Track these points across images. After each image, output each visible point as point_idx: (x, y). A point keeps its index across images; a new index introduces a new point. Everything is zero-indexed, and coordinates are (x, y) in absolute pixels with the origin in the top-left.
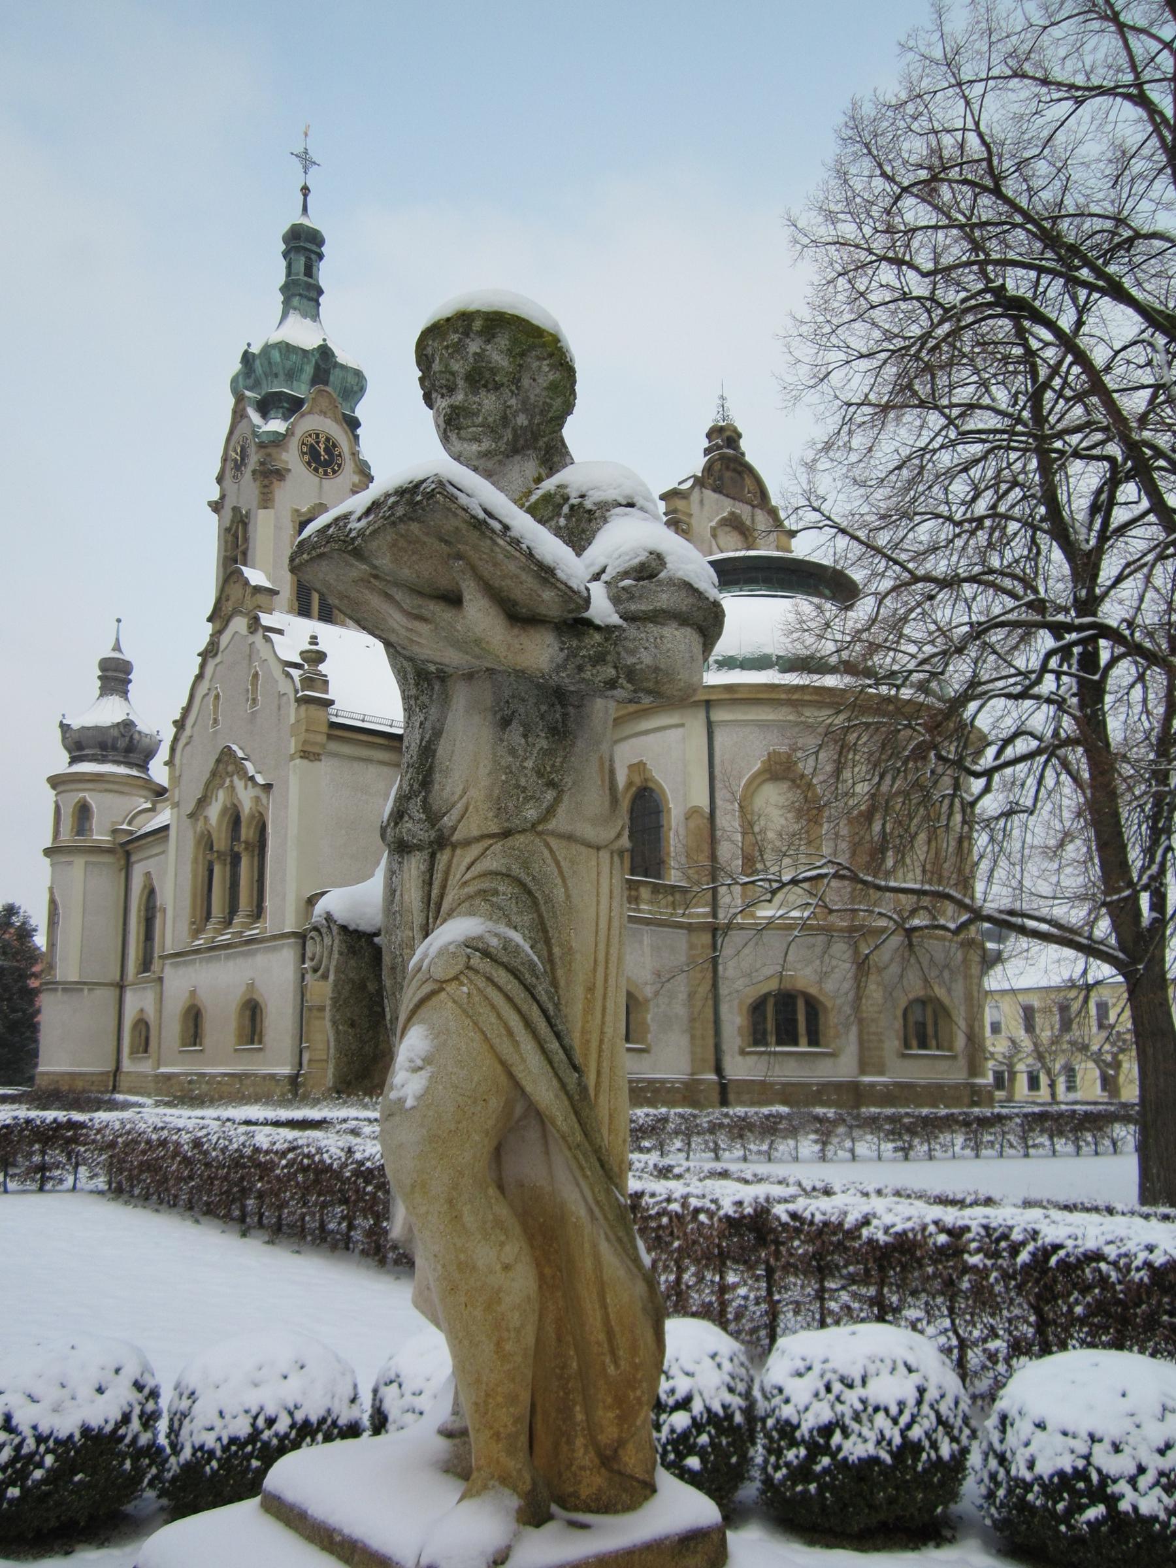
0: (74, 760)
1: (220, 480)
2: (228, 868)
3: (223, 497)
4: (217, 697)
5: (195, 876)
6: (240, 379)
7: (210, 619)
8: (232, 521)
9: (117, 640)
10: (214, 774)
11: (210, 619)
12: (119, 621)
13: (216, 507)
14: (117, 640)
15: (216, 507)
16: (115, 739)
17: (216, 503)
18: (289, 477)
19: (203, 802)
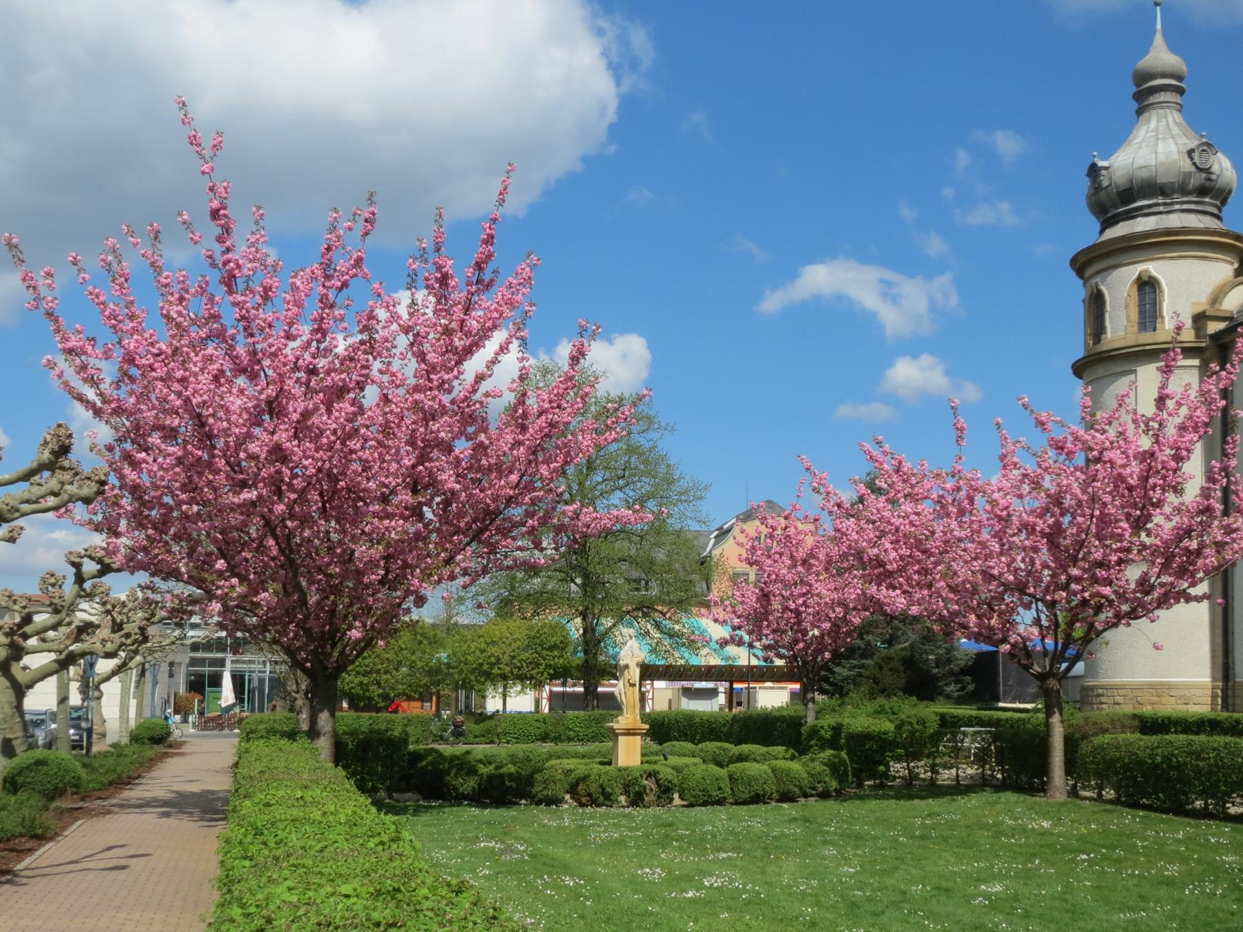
0: (1107, 224)
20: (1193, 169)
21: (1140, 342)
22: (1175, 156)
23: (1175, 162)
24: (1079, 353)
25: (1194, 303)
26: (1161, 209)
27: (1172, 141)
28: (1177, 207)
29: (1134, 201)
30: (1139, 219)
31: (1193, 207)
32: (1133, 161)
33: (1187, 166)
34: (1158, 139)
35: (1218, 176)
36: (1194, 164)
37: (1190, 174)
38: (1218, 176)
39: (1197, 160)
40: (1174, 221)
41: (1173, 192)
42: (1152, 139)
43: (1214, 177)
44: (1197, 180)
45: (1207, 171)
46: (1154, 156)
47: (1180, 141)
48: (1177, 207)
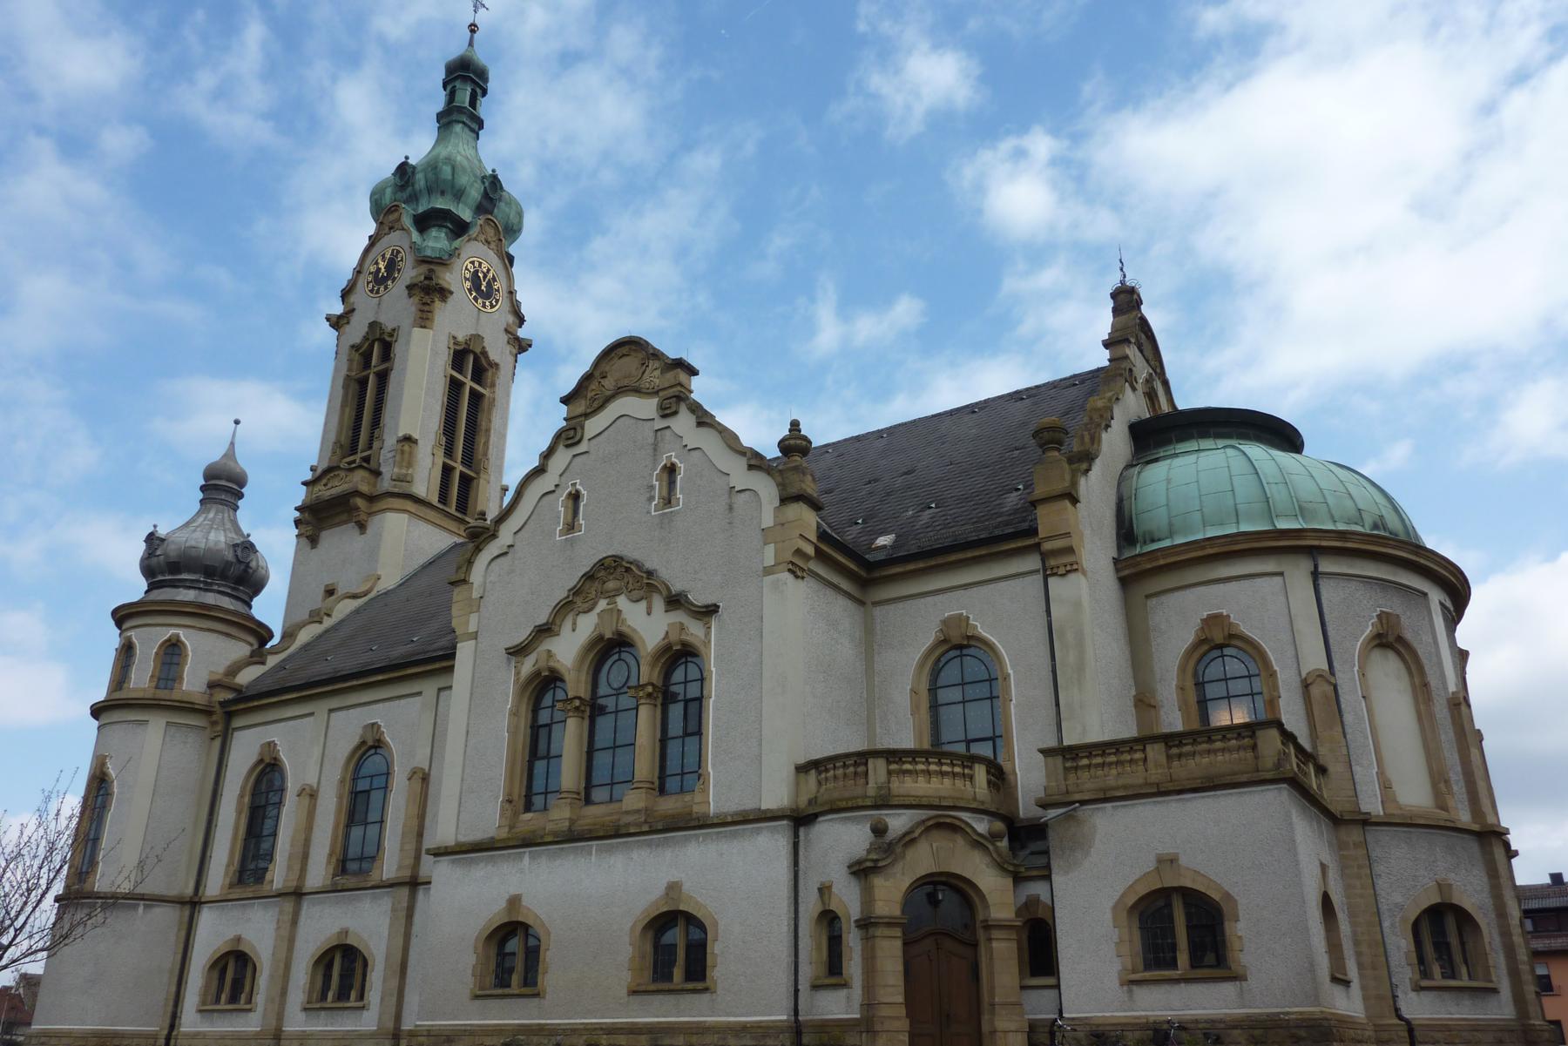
1: (345, 294)
2: (586, 722)
3: (349, 312)
4: (575, 497)
5: (513, 732)
6: (389, 191)
7: (565, 400)
8: (366, 338)
9: (232, 444)
10: (576, 591)
11: (565, 400)
12: (237, 422)
13: (337, 322)
14: (232, 444)
15: (337, 322)
16: (228, 564)
17: (340, 317)
18: (451, 300)
19: (545, 631)
20: (234, 560)
21: (157, 696)
22: (223, 546)
23: (221, 551)
24: (100, 695)
25: (212, 672)
26: (202, 586)
27: (222, 532)
28: (216, 587)
29: (180, 573)
30: (181, 589)
31: (229, 591)
32: (186, 540)
33: (230, 556)
34: (212, 528)
35: (255, 571)
36: (237, 556)
37: (232, 563)
38: (255, 571)
39: (239, 553)
40: (210, 598)
41: (215, 576)
42: (207, 527)
43: (251, 571)
44: (235, 570)
45: (248, 565)
46: (205, 540)
47: (230, 535)
48: (216, 587)
